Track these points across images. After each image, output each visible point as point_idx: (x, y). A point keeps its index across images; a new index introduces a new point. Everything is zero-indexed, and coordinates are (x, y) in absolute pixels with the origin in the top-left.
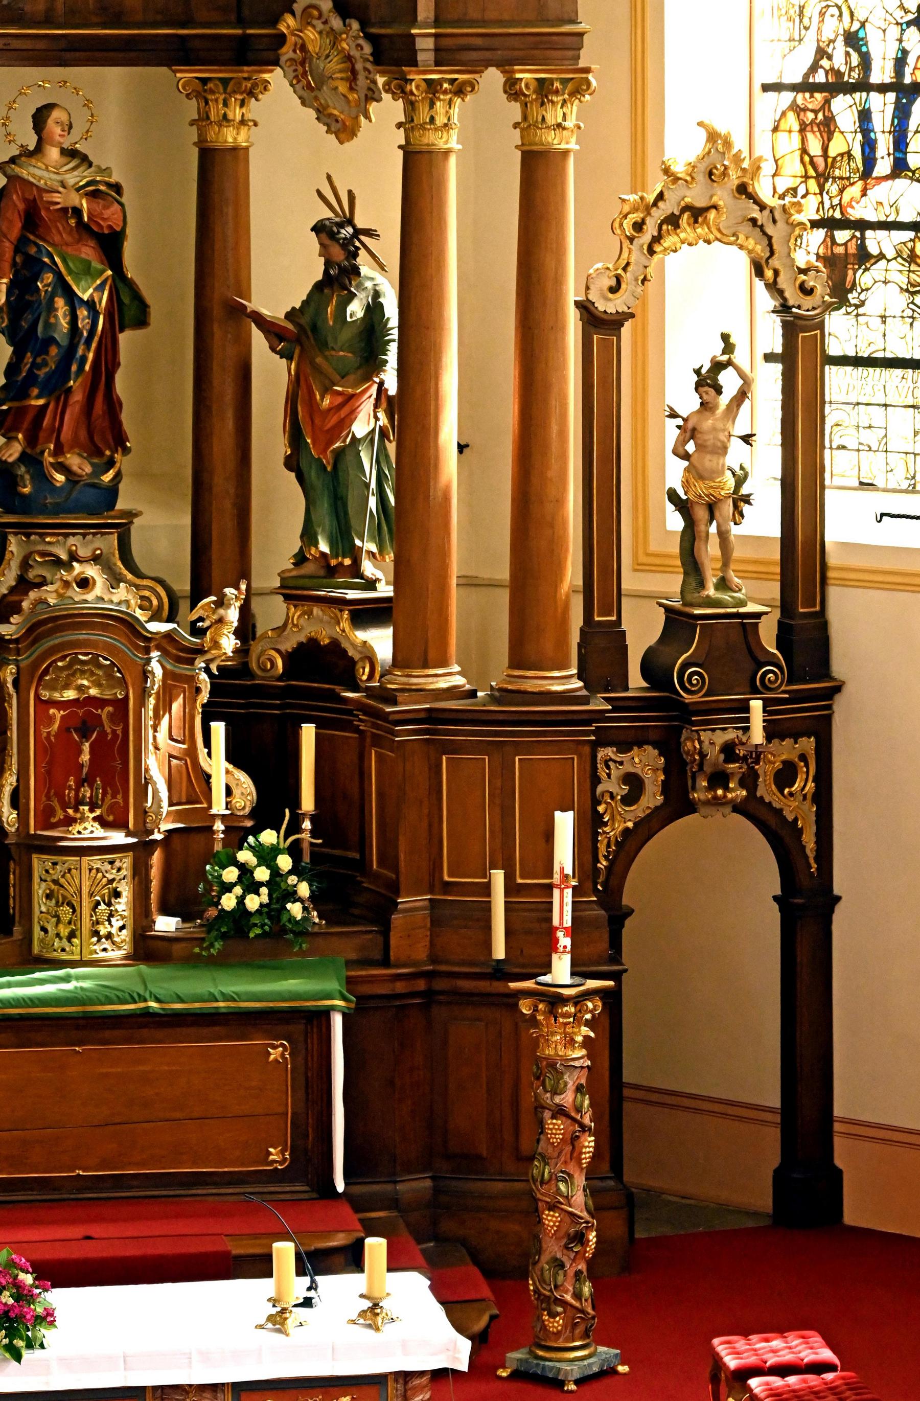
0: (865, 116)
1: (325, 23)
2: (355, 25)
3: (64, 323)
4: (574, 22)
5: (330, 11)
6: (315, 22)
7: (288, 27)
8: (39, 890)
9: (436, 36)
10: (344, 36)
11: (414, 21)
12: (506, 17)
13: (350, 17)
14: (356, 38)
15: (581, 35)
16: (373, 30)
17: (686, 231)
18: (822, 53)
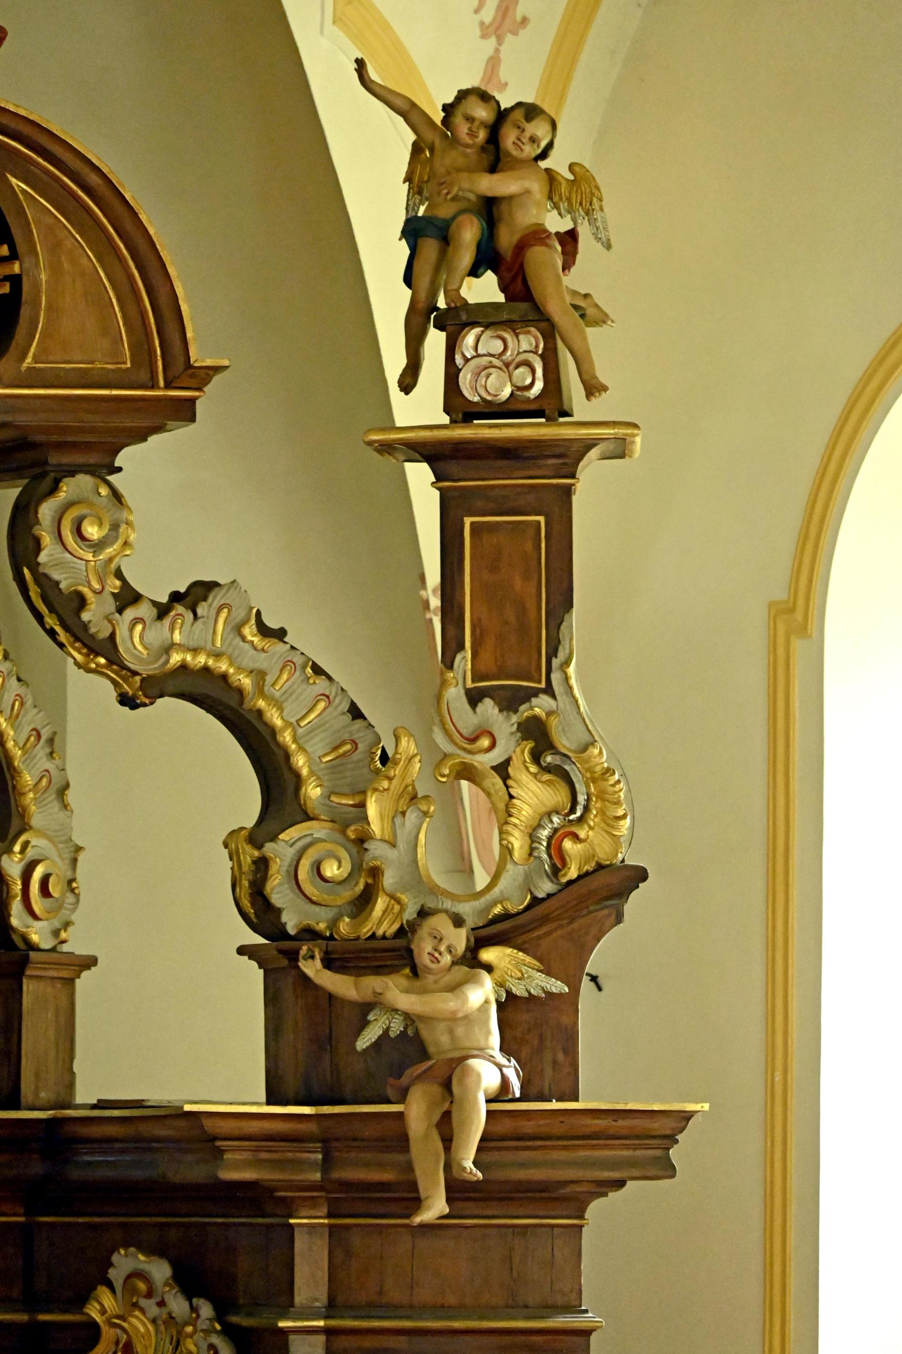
1: (162, 1304)
2: (206, 1310)
4: (575, 1308)
5: (166, 1284)
6: (143, 1302)
7: (103, 1312)
9: (328, 1332)
10: (189, 1329)
11: (287, 1307)
12: (451, 1300)
13: (200, 1296)
14: (207, 1332)
15: (587, 1333)
16: (234, 1319)
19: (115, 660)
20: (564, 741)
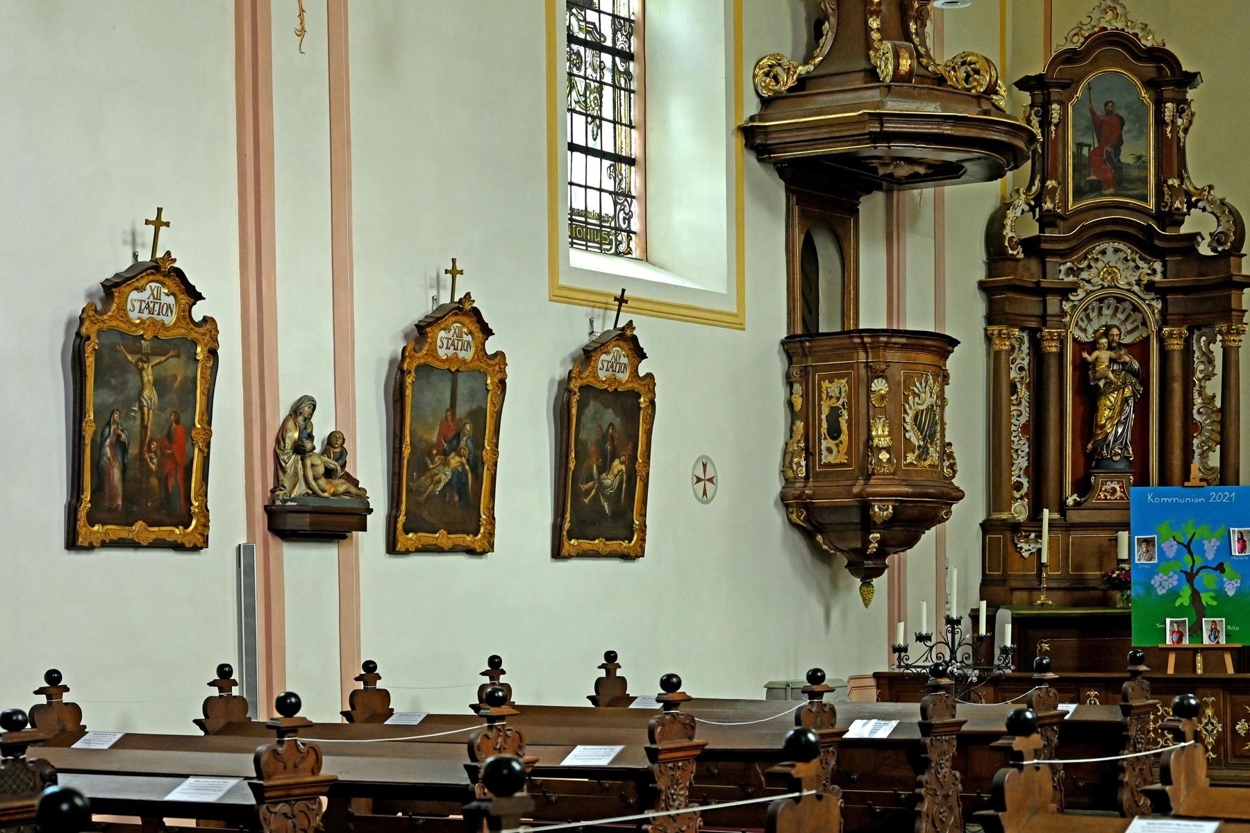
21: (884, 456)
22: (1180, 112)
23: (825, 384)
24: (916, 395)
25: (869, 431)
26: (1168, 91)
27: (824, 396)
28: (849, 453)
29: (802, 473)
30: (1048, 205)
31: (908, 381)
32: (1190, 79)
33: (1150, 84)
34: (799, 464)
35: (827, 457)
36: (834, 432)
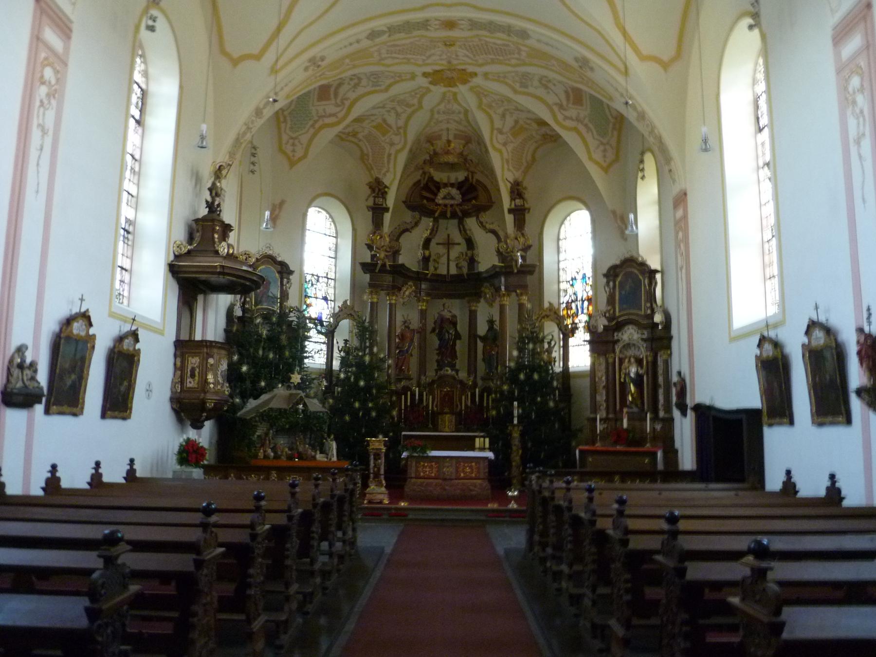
0: (577, 306)
3: (447, 337)
8: (440, 420)
17: (546, 319)
18: (570, 296)
19: (486, 228)
20: (525, 234)
21: (212, 386)
22: (288, 282)
23: (190, 359)
24: (222, 365)
25: (206, 376)
26: (285, 275)
27: (190, 363)
28: (198, 383)
29: (179, 391)
30: (247, 306)
31: (220, 359)
32: (291, 272)
33: (279, 272)
34: (178, 387)
35: (189, 385)
36: (193, 376)
